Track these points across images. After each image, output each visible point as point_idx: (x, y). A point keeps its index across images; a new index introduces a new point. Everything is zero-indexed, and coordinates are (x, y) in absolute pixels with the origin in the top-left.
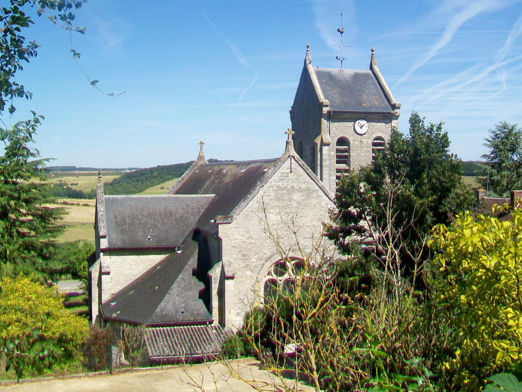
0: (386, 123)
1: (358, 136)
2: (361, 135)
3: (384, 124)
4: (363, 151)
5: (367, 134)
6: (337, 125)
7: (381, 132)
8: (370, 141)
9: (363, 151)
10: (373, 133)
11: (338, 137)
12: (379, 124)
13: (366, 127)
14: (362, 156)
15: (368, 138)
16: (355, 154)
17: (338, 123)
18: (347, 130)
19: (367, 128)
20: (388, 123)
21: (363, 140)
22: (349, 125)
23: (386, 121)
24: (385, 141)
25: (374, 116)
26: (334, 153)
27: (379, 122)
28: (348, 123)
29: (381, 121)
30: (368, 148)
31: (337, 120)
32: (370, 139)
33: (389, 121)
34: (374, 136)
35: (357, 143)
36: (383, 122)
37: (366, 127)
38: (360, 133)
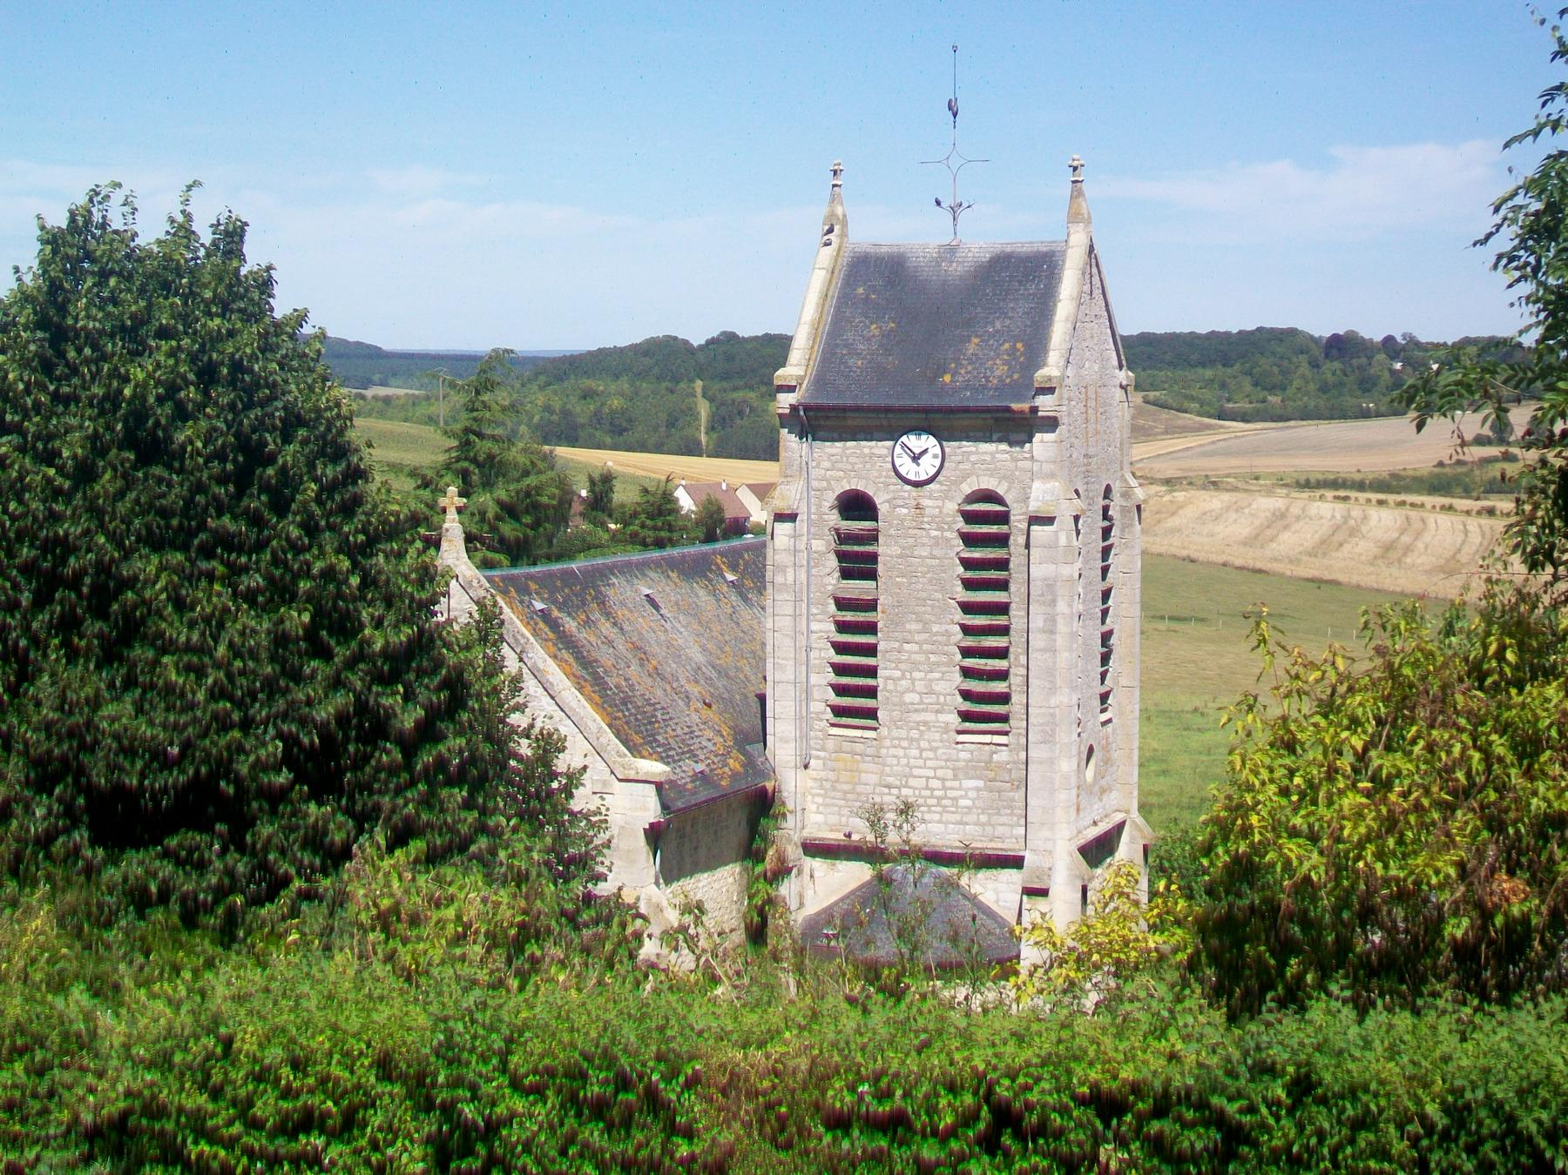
0: (1011, 444)
1: (908, 487)
2: (917, 484)
3: (1004, 446)
5: (941, 483)
6: (834, 451)
8: (952, 507)
9: (925, 540)
10: (964, 478)
11: (839, 491)
13: (935, 456)
15: (946, 496)
16: (896, 550)
17: (838, 444)
18: (868, 466)
19: (938, 462)
20: (1021, 444)
21: (926, 502)
22: (876, 451)
23: (1014, 437)
24: (1005, 505)
26: (823, 545)
27: (989, 440)
28: (873, 443)
29: (995, 437)
30: (940, 529)
31: (835, 435)
32: (951, 499)
33: (1023, 436)
34: (967, 488)
35: (905, 511)
36: (1000, 441)
37: (935, 456)
38: (911, 477)
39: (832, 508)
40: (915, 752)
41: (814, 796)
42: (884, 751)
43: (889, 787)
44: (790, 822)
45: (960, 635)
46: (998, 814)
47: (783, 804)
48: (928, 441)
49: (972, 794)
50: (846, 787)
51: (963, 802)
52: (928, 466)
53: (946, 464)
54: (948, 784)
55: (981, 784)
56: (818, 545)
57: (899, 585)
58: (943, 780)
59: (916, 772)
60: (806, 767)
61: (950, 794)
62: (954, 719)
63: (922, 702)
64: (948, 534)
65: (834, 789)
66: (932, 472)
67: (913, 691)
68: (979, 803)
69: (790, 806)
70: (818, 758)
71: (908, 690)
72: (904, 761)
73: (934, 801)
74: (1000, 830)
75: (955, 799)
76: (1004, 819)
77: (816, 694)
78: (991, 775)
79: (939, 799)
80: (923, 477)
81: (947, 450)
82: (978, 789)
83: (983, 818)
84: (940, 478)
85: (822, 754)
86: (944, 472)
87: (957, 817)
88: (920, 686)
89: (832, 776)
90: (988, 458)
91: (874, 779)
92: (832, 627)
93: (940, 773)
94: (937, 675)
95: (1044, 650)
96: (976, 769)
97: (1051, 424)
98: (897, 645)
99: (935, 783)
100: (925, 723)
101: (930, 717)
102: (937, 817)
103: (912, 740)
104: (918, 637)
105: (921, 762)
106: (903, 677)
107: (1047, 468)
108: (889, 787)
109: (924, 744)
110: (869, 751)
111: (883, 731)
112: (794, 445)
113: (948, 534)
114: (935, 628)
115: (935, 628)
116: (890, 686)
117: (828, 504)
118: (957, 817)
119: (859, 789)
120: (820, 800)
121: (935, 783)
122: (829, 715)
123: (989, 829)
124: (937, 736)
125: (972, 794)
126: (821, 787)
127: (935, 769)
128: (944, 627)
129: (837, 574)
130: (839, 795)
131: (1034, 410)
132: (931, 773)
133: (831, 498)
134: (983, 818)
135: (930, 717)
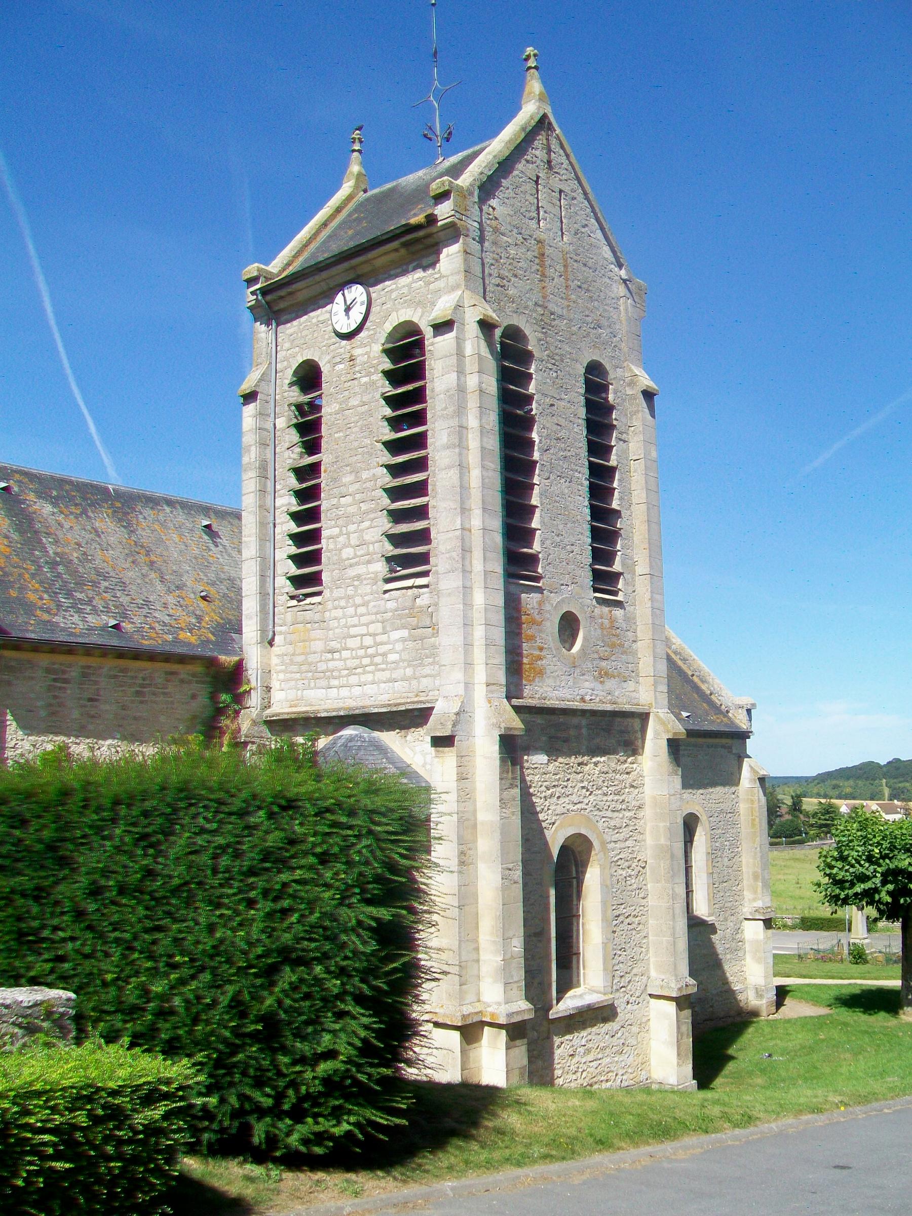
0: (425, 269)
1: (344, 342)
3: (419, 274)
4: (357, 389)
6: (289, 331)
7: (409, 307)
8: (377, 348)
9: (357, 389)
12: (403, 281)
13: (362, 304)
14: (354, 407)
15: (372, 339)
16: (335, 407)
17: (295, 323)
19: (363, 309)
20: (433, 265)
21: (357, 352)
22: (321, 318)
23: (425, 262)
25: (380, 257)
26: (284, 420)
27: (405, 273)
29: (411, 267)
30: (369, 374)
34: (389, 327)
35: (341, 366)
36: (414, 269)
39: (291, 384)
40: (351, 611)
41: (278, 672)
42: (327, 614)
43: (332, 652)
44: (254, 700)
45: (388, 478)
46: (422, 665)
47: (249, 682)
48: (357, 292)
49: (399, 646)
50: (300, 659)
51: (393, 657)
52: (357, 315)
53: (373, 309)
54: (379, 639)
55: (404, 633)
56: (281, 423)
57: (337, 441)
58: (375, 635)
59: (353, 631)
60: (271, 643)
61: (382, 649)
62: (381, 568)
63: (356, 556)
64: (374, 377)
65: (292, 663)
66: (359, 320)
67: (349, 546)
68: (405, 656)
69: (253, 684)
70: (281, 633)
71: (345, 546)
72: (343, 621)
73: (366, 661)
74: (425, 682)
75: (384, 655)
76: (427, 670)
77: (280, 570)
78: (414, 621)
79: (372, 656)
80: (353, 326)
81: (374, 296)
82: (403, 640)
83: (409, 672)
84: (368, 324)
85: (283, 629)
86: (371, 318)
87: (387, 674)
88: (354, 540)
89: (290, 649)
90: (405, 290)
91: (318, 646)
92: (294, 501)
93: (371, 630)
94: (367, 524)
95: (449, 467)
96: (400, 617)
97: (453, 232)
98: (335, 501)
99: (368, 641)
100: (358, 577)
101: (361, 570)
102: (370, 677)
103: (349, 597)
104: (352, 489)
105: (355, 620)
106: (341, 534)
107: (452, 280)
108: (332, 652)
109: (358, 600)
110: (317, 617)
111: (327, 593)
112: (263, 335)
113: (374, 377)
114: (365, 475)
115: (365, 475)
116: (331, 546)
117: (287, 382)
118: (387, 674)
119: (312, 658)
120: (281, 676)
121: (368, 641)
122: (289, 588)
123: (414, 682)
124: (368, 589)
125: (399, 646)
126: (283, 663)
127: (367, 625)
128: (372, 471)
129: (298, 450)
130: (294, 668)
131: (431, 219)
132: (363, 630)
133: (288, 375)
134: (409, 672)
135: (361, 570)
